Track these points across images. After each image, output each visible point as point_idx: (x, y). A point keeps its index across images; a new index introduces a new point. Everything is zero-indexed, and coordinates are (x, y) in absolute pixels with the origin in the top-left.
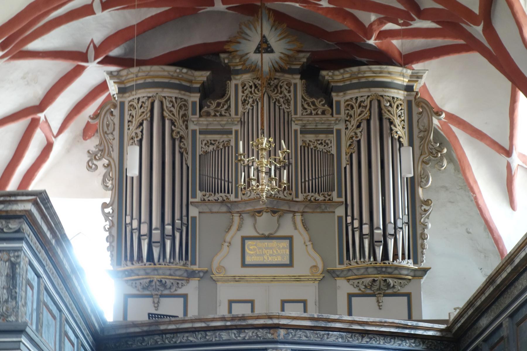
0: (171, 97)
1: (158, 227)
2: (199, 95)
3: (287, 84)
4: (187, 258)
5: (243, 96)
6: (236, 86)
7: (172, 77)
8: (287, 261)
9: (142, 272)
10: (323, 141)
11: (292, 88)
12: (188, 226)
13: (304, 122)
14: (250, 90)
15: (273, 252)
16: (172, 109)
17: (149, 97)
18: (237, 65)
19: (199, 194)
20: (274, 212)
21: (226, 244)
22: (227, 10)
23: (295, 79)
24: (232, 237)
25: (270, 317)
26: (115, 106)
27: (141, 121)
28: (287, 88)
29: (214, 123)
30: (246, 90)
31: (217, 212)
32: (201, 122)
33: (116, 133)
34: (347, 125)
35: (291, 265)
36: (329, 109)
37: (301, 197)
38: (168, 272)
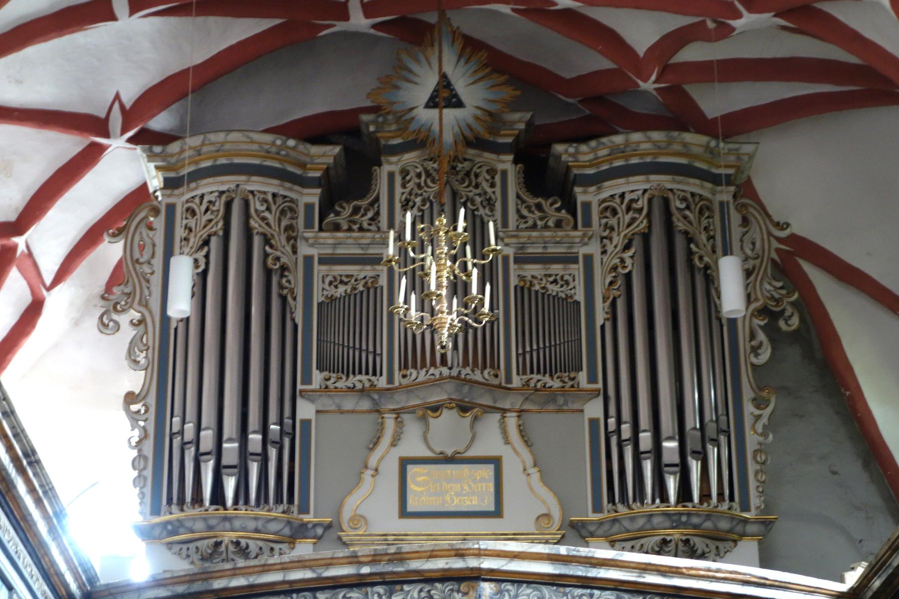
0: (265, 193)
1: (234, 436)
2: (319, 191)
3: (488, 172)
4: (291, 500)
5: (403, 193)
6: (391, 175)
7: (268, 155)
8: (489, 505)
9: (200, 525)
10: (558, 277)
11: (498, 179)
12: (293, 438)
13: (522, 240)
15: (462, 488)
16: (266, 214)
17: (222, 193)
18: (393, 137)
19: (318, 377)
20: (464, 409)
21: (370, 472)
22: (372, 31)
23: (503, 162)
24: (382, 458)
25: (460, 554)
26: (156, 211)
27: (205, 236)
28: (488, 177)
29: (349, 244)
30: (409, 181)
31: (353, 412)
32: (322, 241)
33: (158, 262)
34: (604, 246)
35: (497, 513)
36: (570, 217)
37: (517, 381)
38: (252, 525)
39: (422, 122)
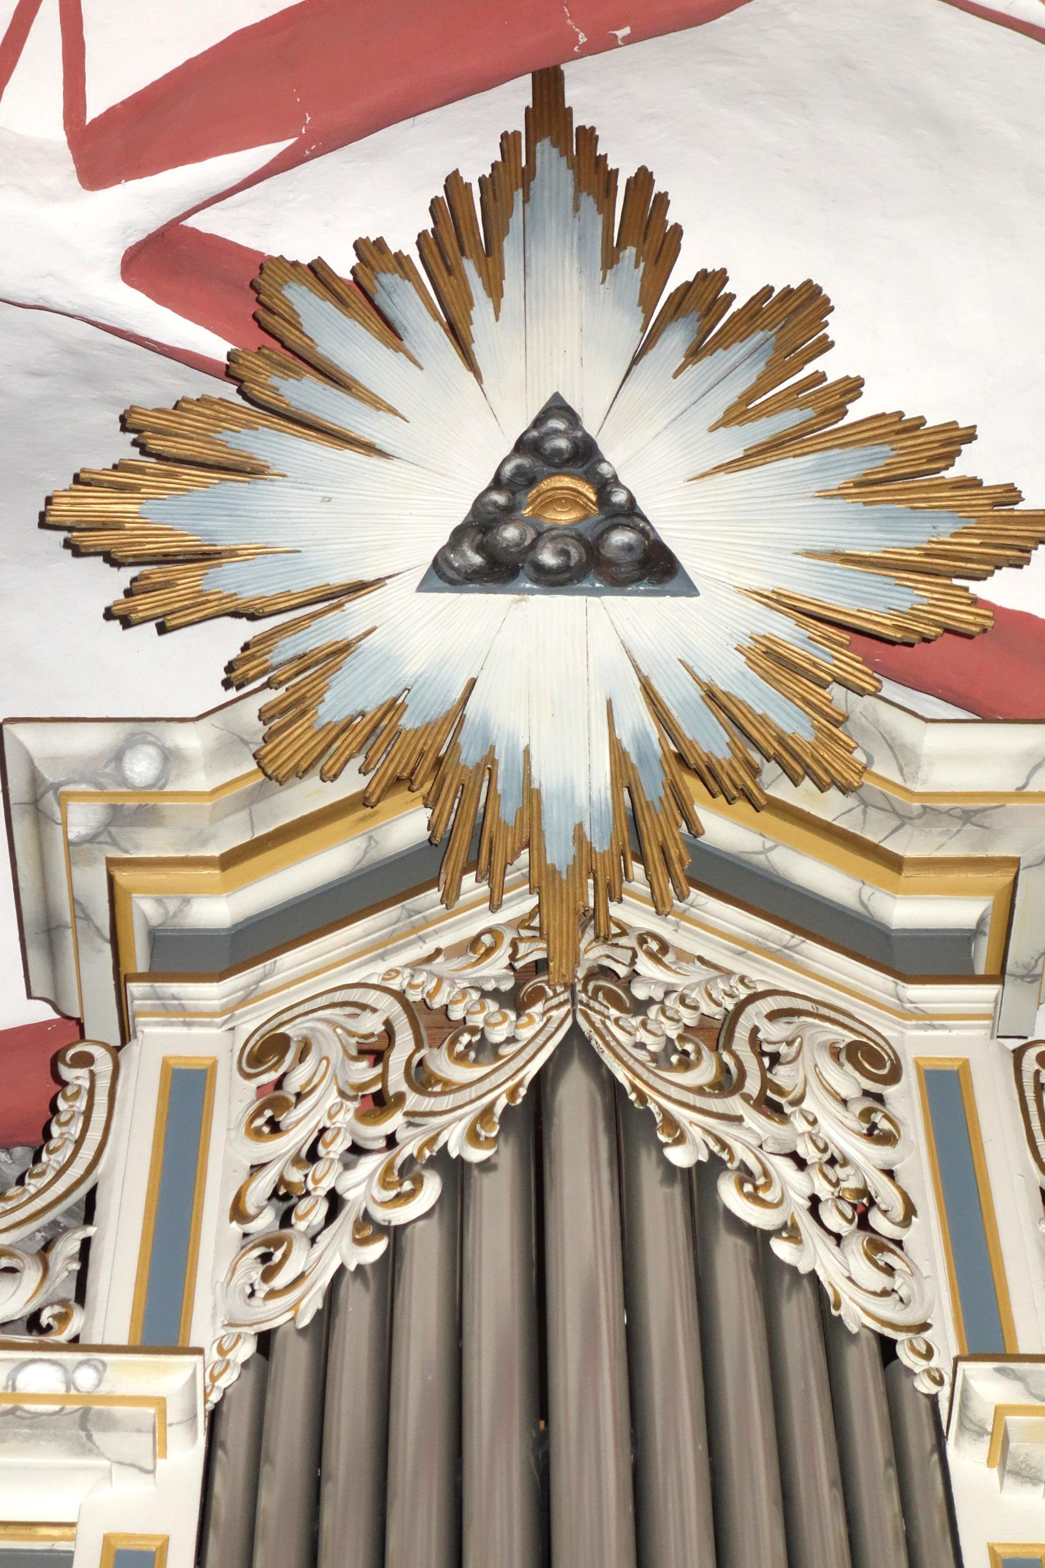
5: (257, 1168)
6: (186, 1093)
11: (905, 1101)
14: (363, 1071)
39: (412, 668)
